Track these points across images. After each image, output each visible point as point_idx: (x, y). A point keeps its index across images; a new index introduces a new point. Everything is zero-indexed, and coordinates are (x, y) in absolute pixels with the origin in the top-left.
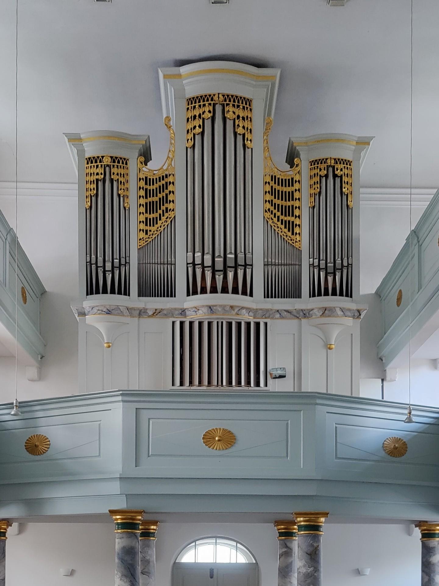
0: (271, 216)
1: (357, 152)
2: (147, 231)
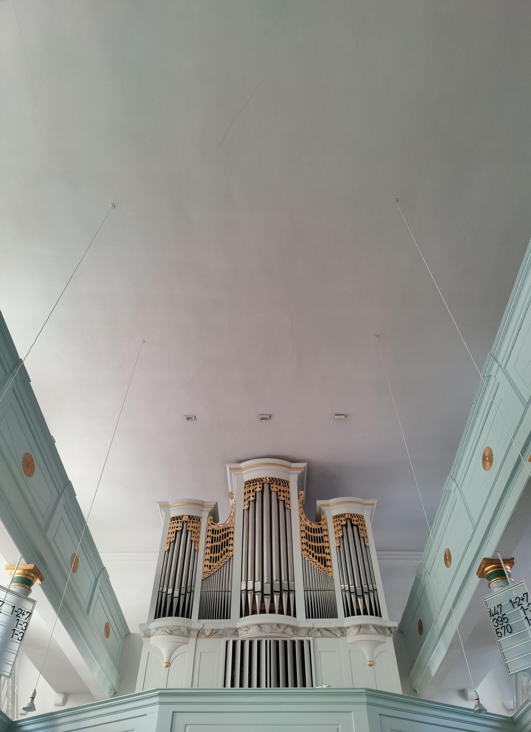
0: (307, 553)
2: (210, 566)
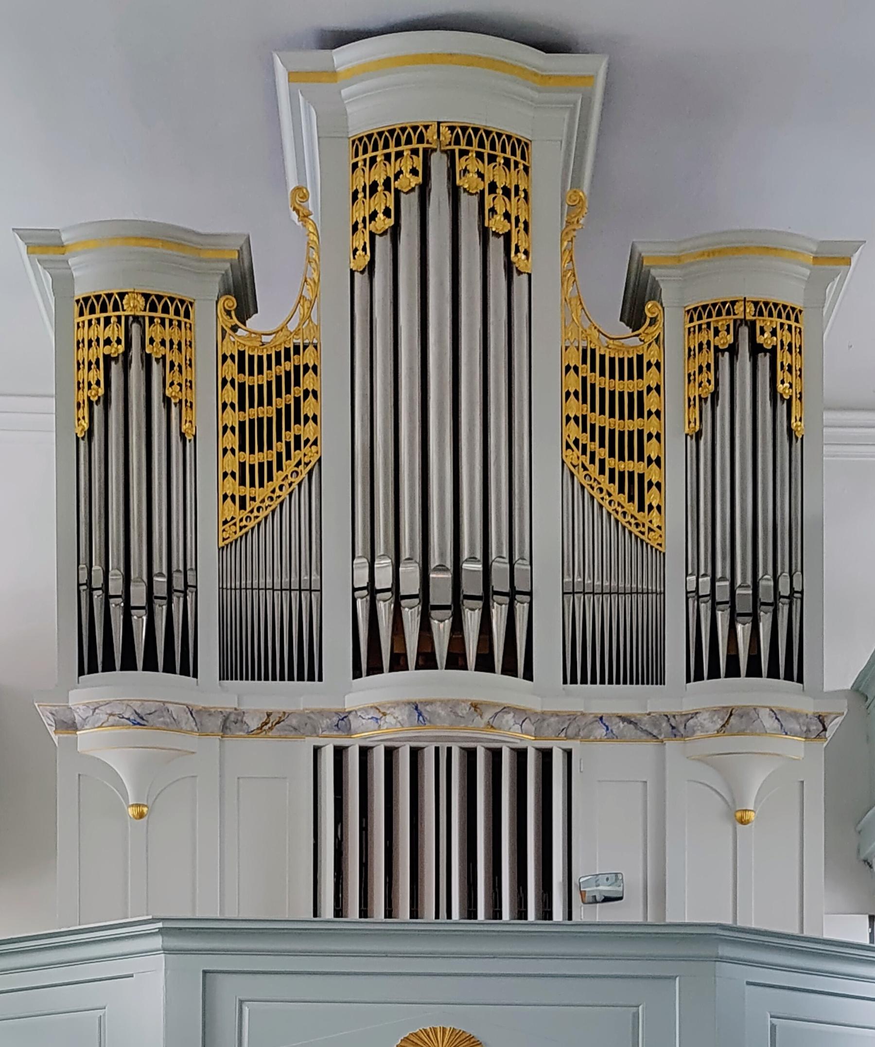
0: (583, 458)
2: (243, 499)
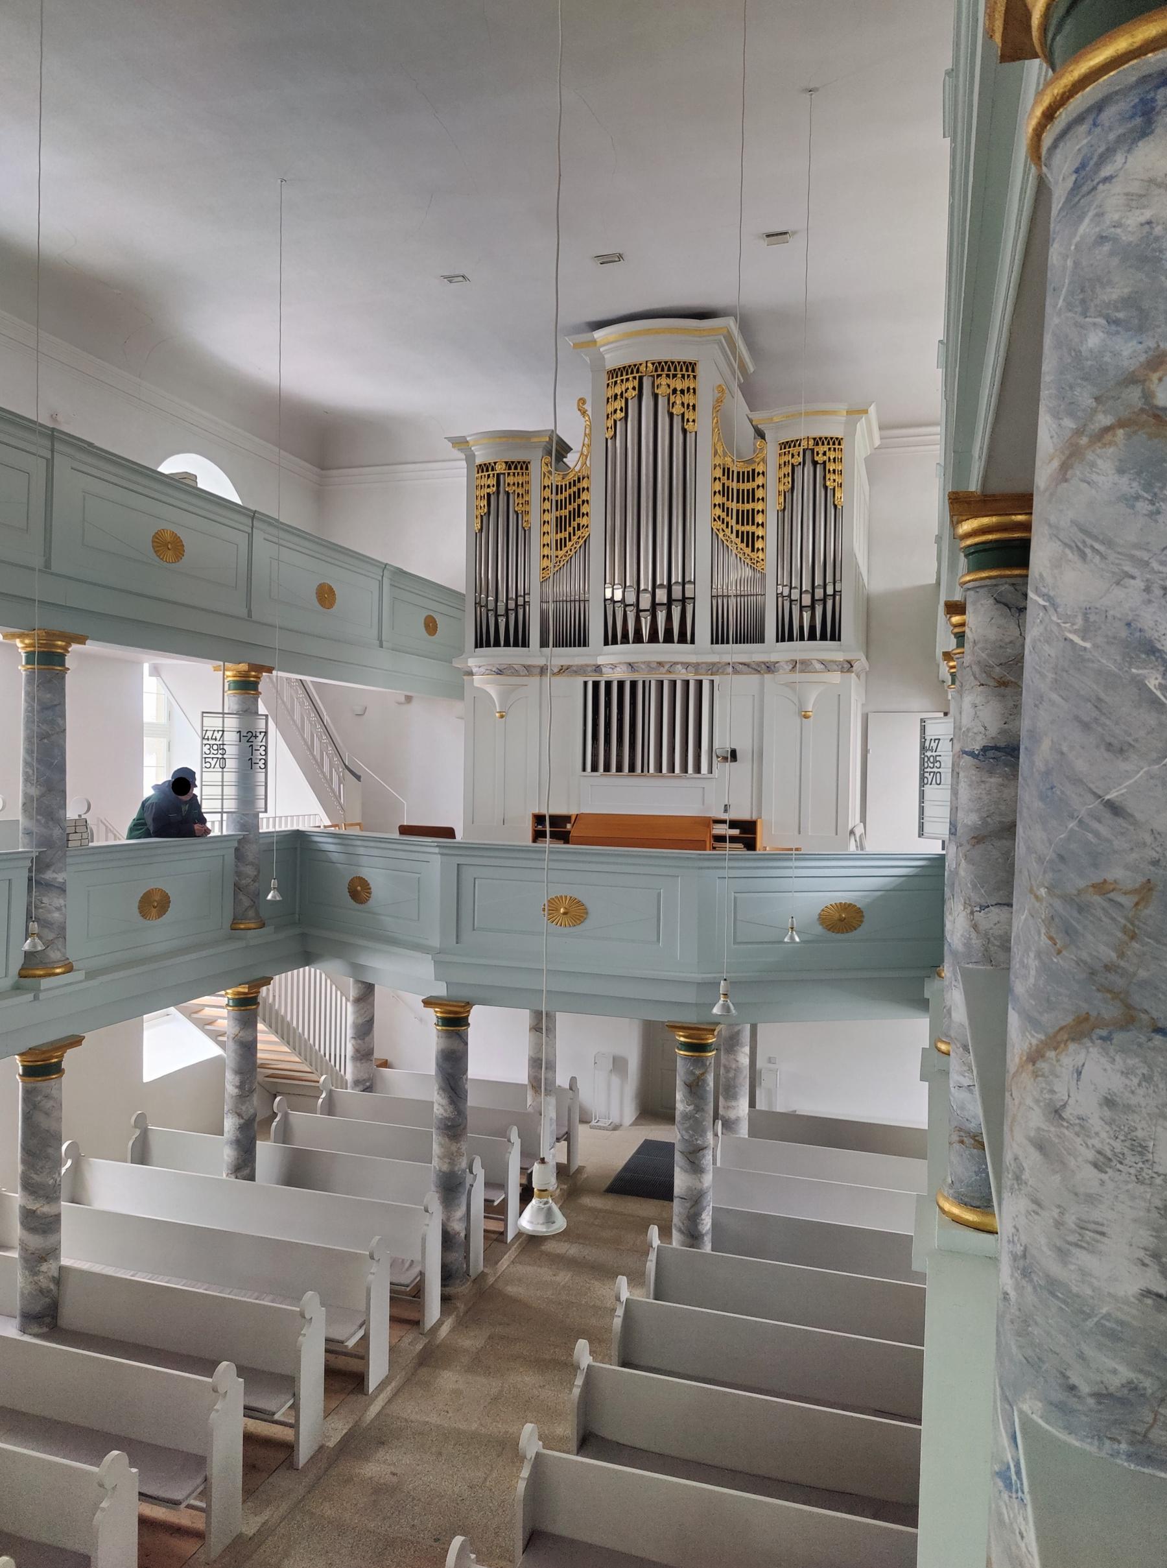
0: (722, 526)
1: (851, 426)
